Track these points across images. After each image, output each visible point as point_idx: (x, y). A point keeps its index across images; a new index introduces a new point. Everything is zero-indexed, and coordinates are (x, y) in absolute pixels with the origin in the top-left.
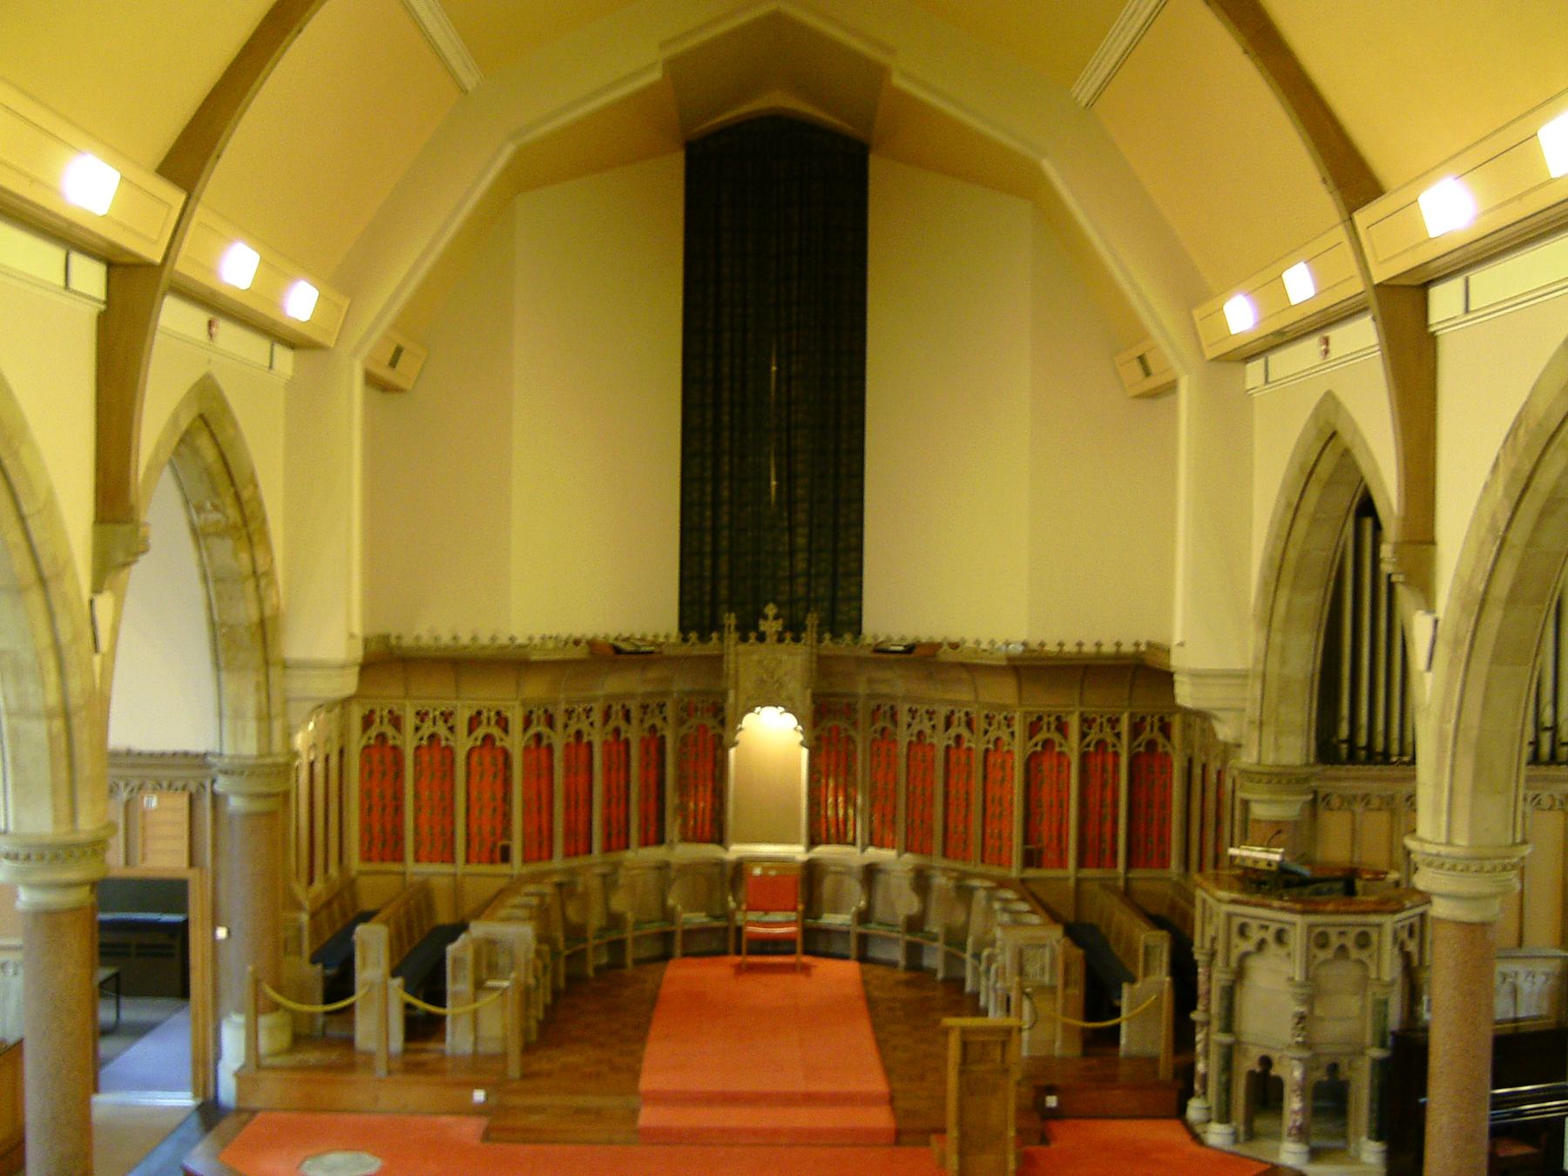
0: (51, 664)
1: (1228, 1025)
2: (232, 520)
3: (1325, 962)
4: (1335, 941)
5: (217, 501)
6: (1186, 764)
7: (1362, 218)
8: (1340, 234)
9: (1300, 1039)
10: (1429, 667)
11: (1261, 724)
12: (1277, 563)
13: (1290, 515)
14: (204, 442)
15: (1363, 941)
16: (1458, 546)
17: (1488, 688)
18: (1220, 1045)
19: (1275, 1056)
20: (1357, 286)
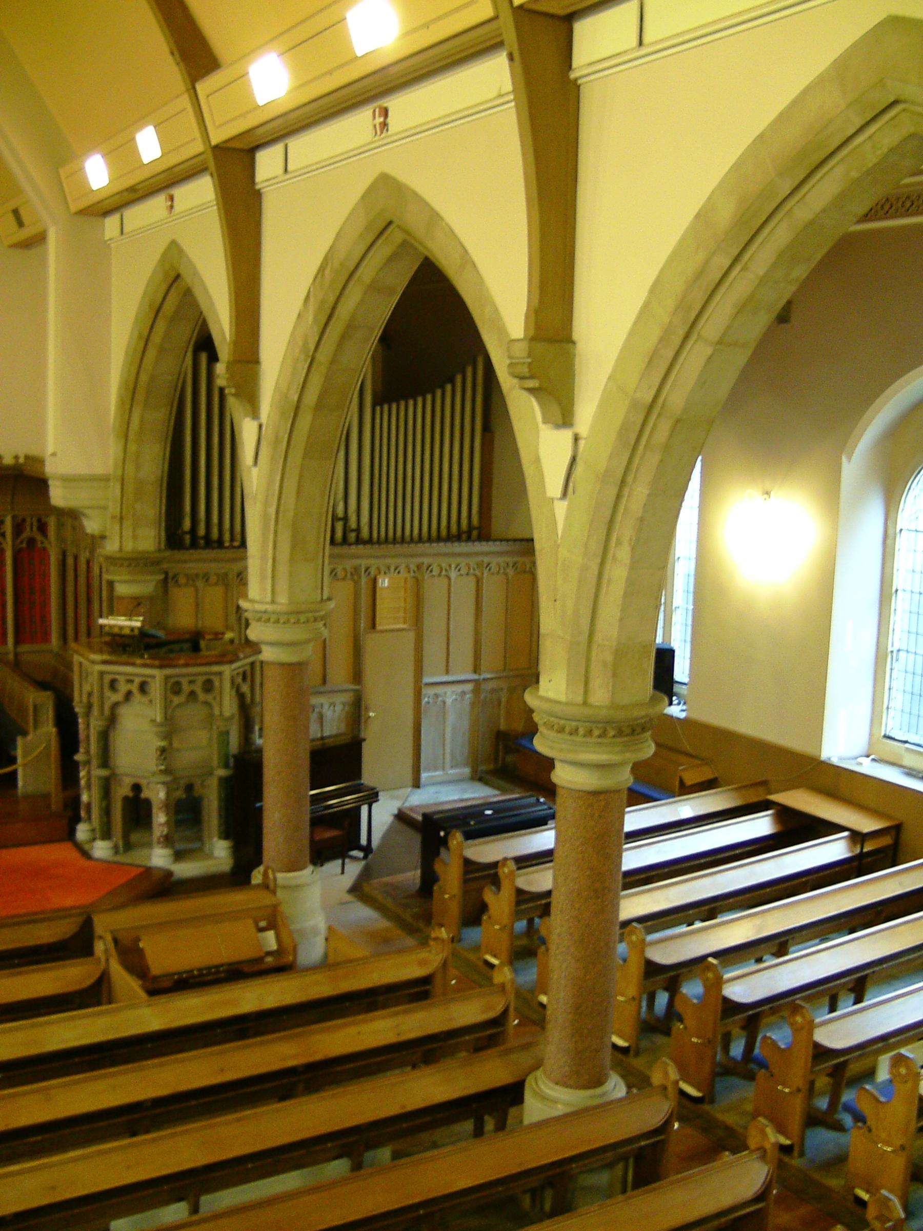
1: (105, 762)
3: (178, 706)
4: (186, 688)
6: (61, 557)
7: (202, 88)
8: (185, 101)
9: (163, 767)
11: (121, 518)
12: (132, 386)
13: (142, 345)
15: (208, 686)
18: (100, 778)
19: (143, 782)
20: (198, 147)
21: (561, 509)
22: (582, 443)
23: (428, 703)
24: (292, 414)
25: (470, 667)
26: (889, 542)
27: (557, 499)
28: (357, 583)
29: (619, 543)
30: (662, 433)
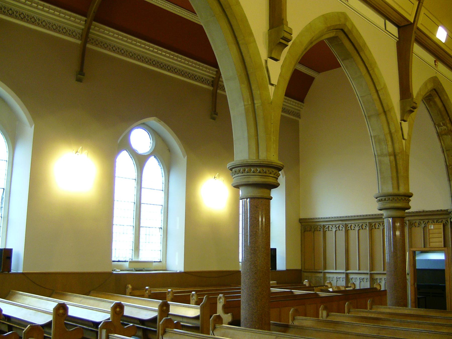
0: (389, 139)
2: (449, 129)
5: (444, 122)
14: (437, 100)
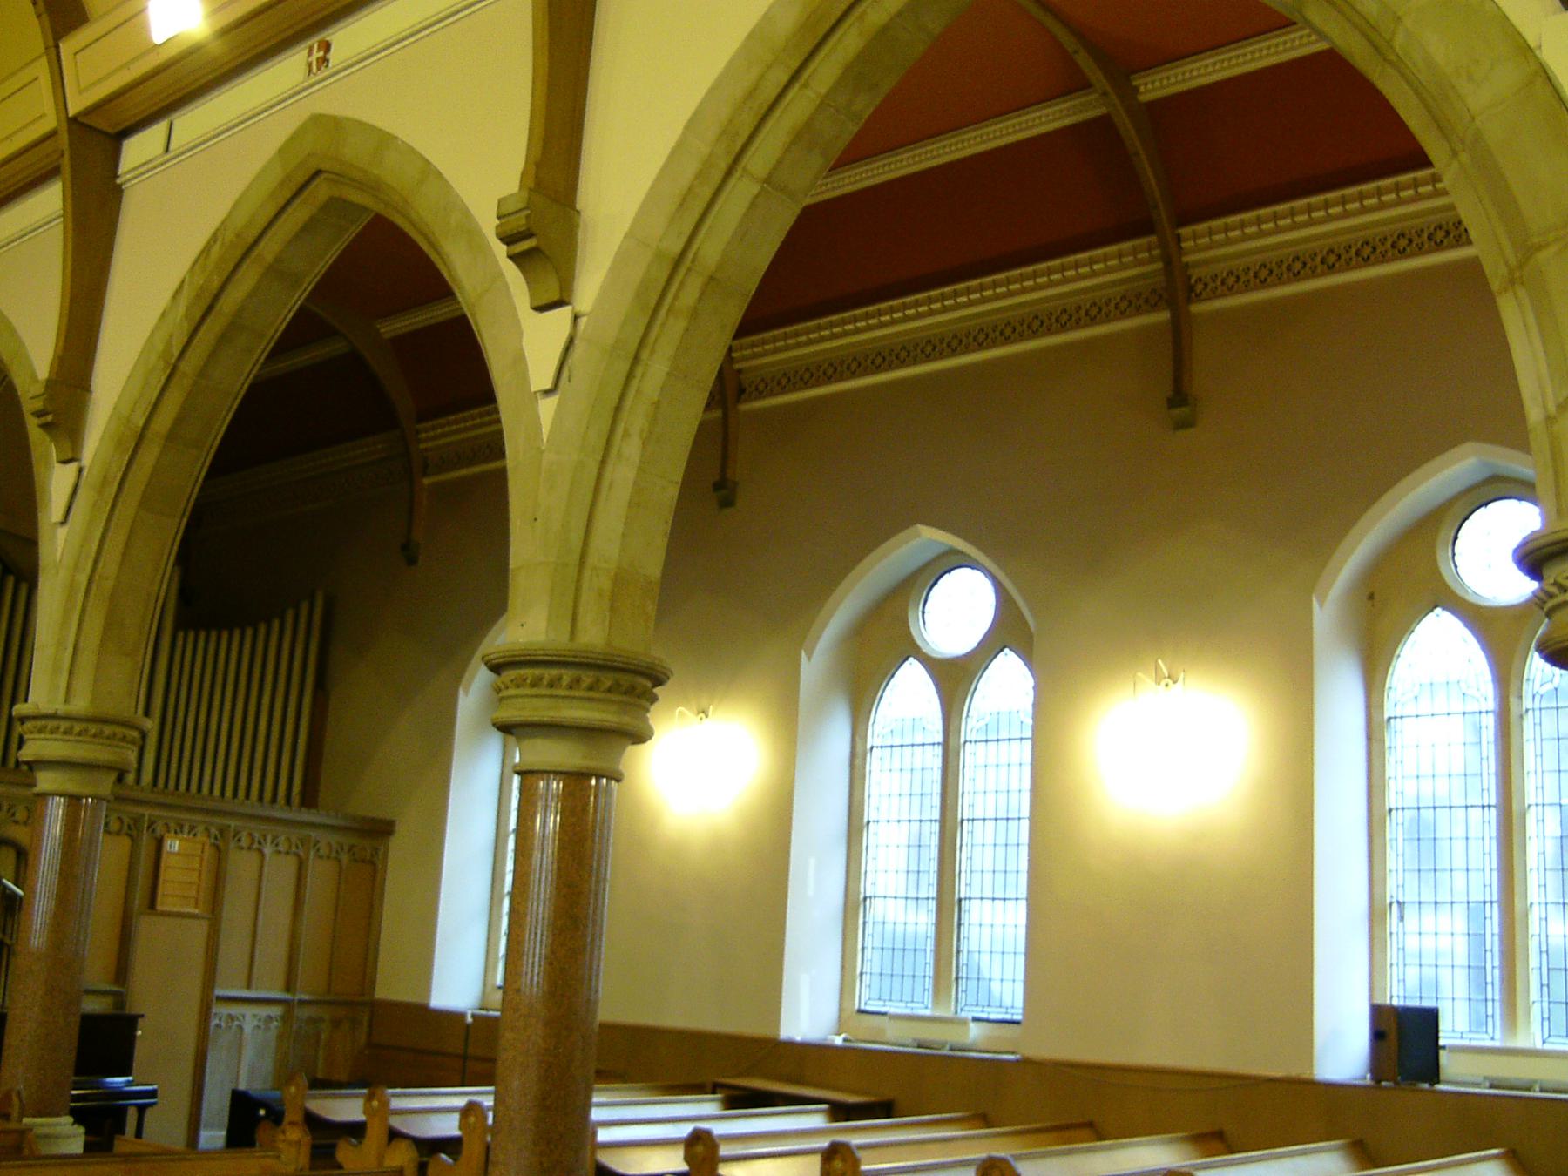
8: (42, 69)
10: (63, 523)
16: (121, 379)
17: (132, 532)
21: (547, 409)
22: (583, 322)
23: (218, 1026)
24: (133, 444)
25: (281, 979)
26: (858, 762)
27: (573, 308)
28: (135, 841)
29: (626, 434)
30: (690, 296)
